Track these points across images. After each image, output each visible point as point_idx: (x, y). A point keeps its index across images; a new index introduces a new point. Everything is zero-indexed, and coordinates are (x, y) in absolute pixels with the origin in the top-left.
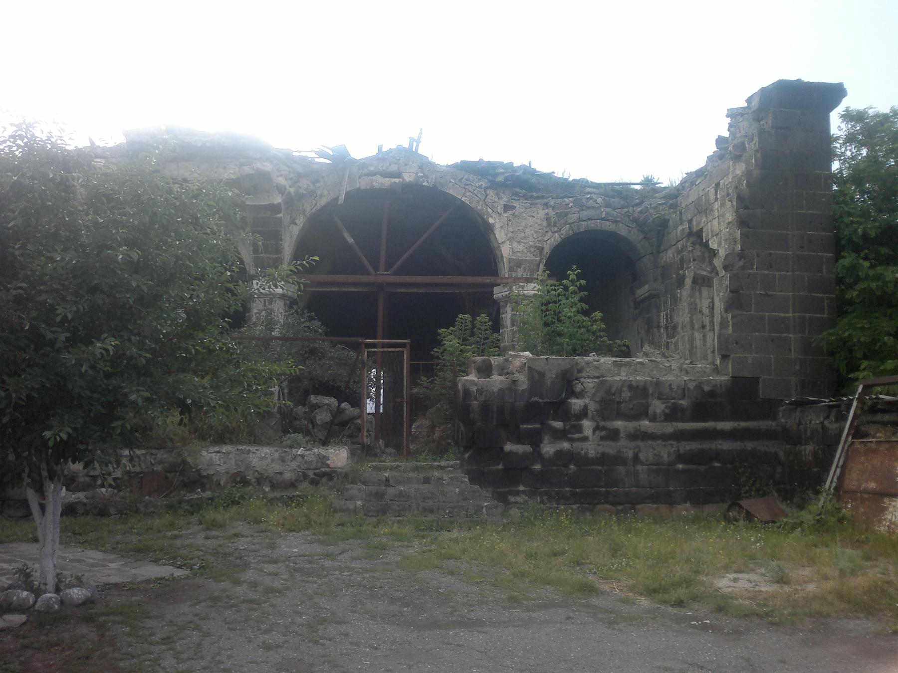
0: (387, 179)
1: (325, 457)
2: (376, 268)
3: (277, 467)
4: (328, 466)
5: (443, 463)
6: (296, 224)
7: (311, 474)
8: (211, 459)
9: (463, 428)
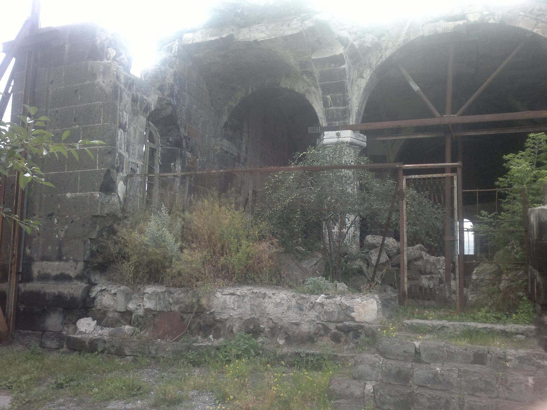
0: (450, 23)
1: (348, 308)
2: (442, 112)
3: (293, 316)
4: (353, 319)
5: (510, 327)
6: (363, 78)
7: (332, 327)
8: (225, 302)
9: (539, 279)
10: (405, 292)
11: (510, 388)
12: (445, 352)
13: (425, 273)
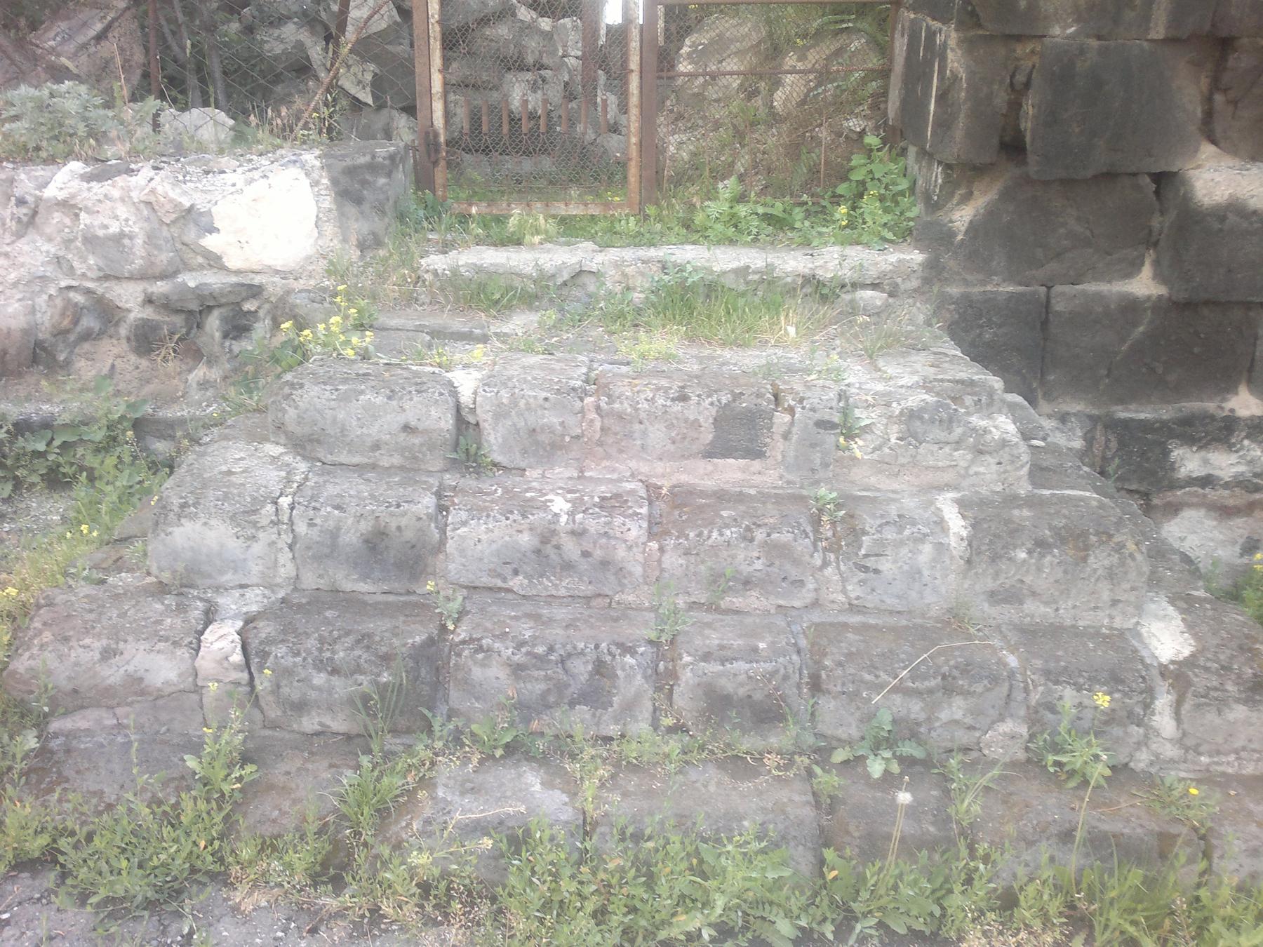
1: (188, 214)
4: (214, 261)
5: (832, 259)
7: (128, 296)
9: (956, 61)
10: (436, 135)
11: (870, 562)
12: (593, 415)
13: (523, 68)
